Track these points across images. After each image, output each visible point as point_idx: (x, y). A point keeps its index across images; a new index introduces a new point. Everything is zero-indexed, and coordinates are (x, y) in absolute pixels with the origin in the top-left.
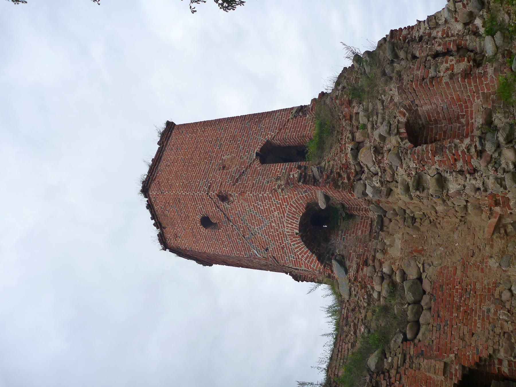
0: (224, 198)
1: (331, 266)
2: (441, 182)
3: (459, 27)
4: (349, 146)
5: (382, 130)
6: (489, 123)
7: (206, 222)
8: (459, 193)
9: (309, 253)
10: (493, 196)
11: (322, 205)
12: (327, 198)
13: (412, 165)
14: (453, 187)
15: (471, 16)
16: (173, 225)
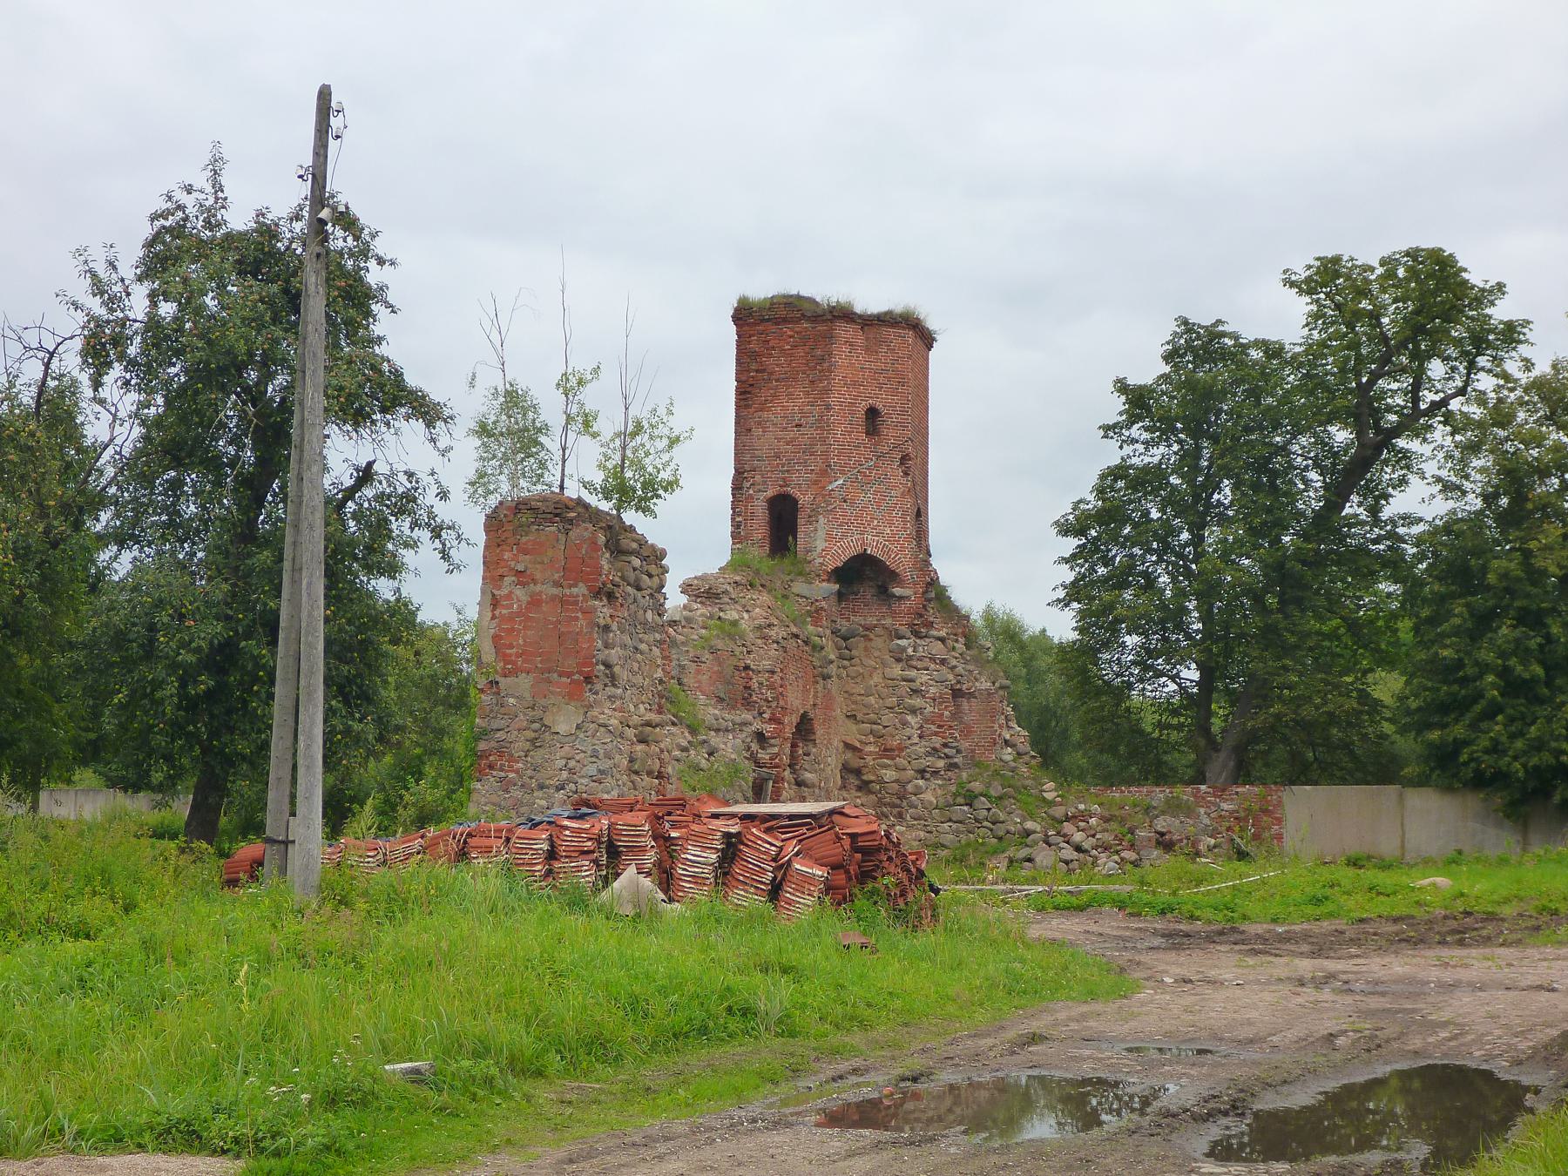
0: (904, 459)
1: (828, 581)
2: (914, 711)
3: (1008, 737)
4: (943, 633)
5: (960, 669)
6: (958, 751)
7: (872, 413)
8: (905, 724)
9: (844, 558)
10: (901, 749)
11: (897, 591)
12: (901, 598)
13: (933, 690)
14: (909, 718)
15: (1013, 746)
16: (867, 350)
